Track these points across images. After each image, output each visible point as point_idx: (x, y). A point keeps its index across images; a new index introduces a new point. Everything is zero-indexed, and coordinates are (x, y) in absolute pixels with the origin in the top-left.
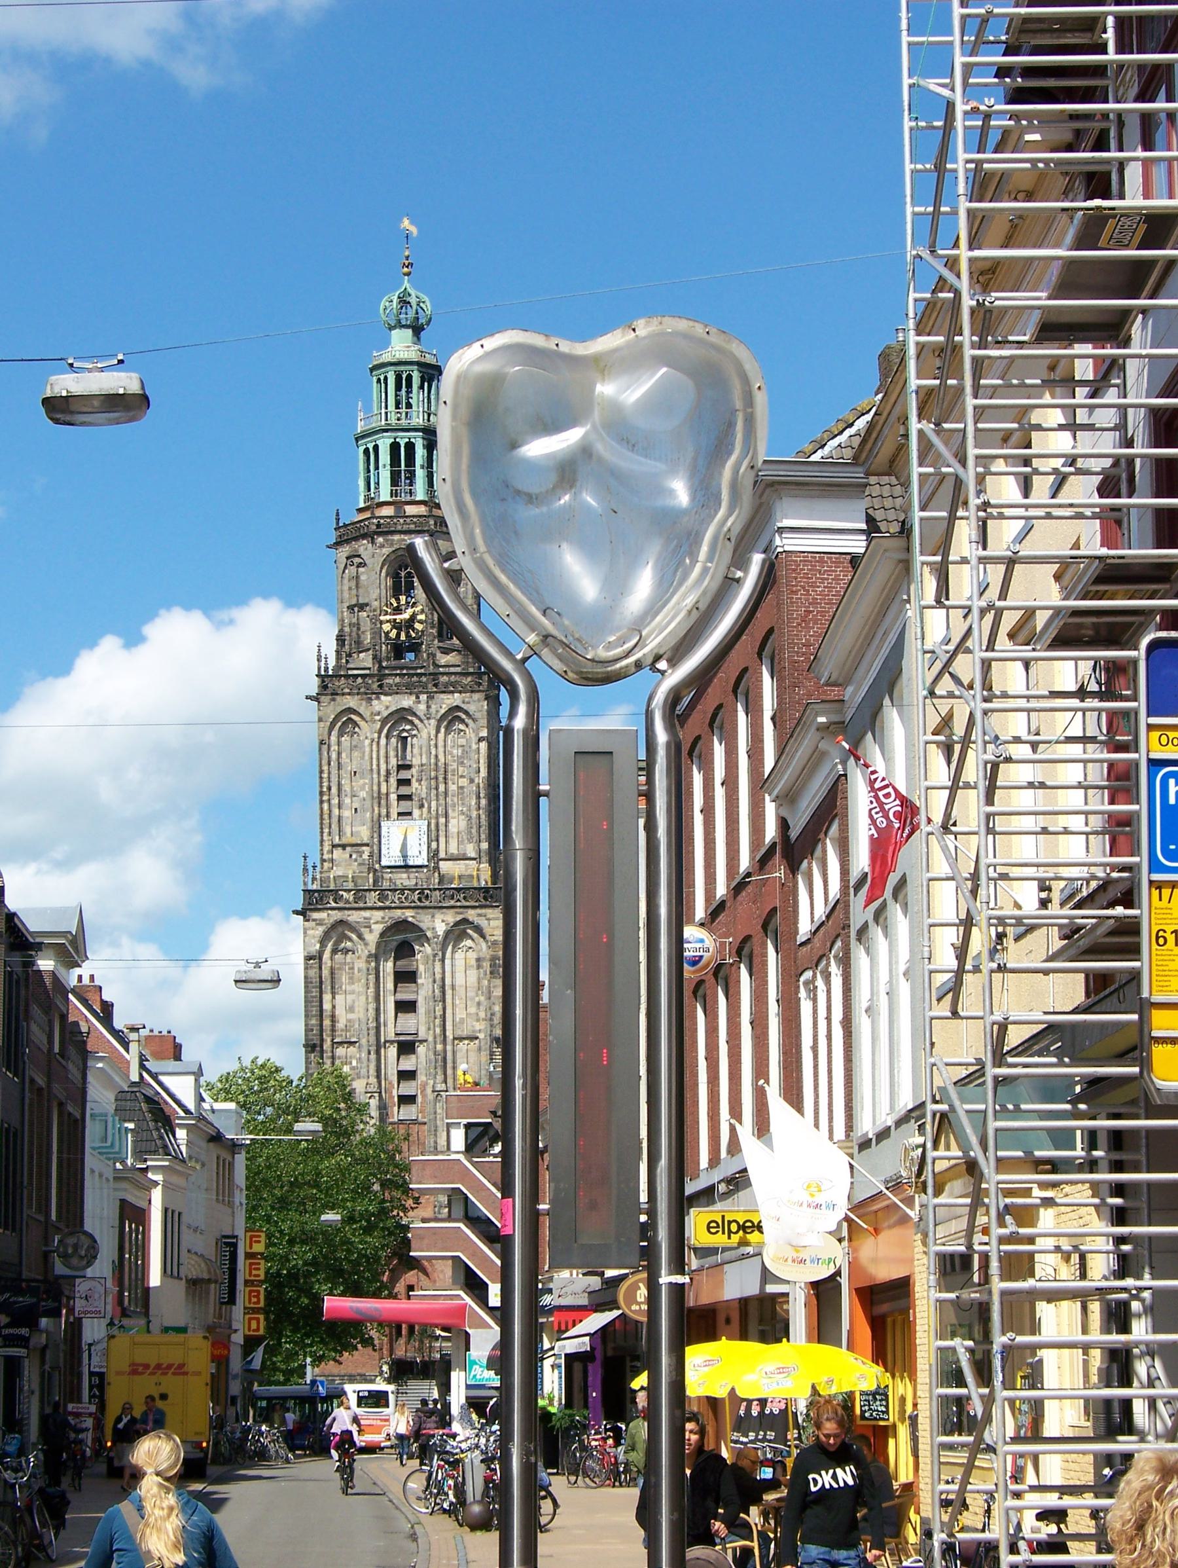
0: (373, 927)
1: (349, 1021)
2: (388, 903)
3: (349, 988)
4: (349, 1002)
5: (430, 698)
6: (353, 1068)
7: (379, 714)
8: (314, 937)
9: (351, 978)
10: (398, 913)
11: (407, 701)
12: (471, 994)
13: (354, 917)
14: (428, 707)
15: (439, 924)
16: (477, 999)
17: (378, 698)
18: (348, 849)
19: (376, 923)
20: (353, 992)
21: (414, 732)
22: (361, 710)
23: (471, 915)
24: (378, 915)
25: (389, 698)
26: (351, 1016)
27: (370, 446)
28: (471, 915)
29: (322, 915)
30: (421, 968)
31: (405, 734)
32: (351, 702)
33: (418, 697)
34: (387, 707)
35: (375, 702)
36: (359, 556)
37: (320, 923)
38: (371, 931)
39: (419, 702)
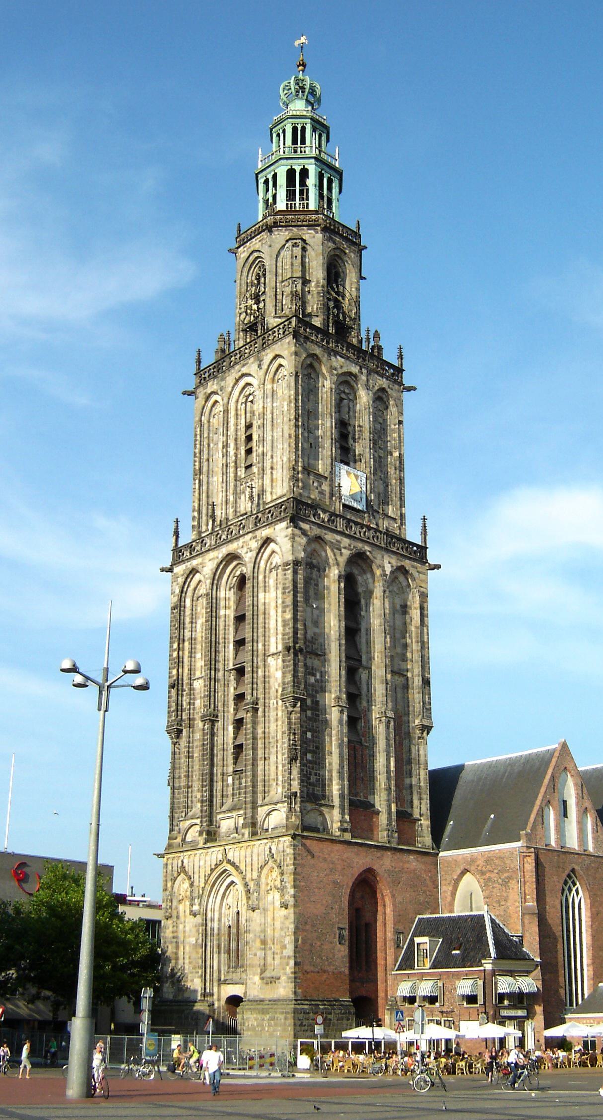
0: (343, 550)
2: (352, 533)
5: (368, 374)
6: (317, 680)
7: (336, 369)
8: (300, 544)
11: (355, 369)
13: (329, 537)
14: (367, 380)
15: (387, 564)
17: (335, 356)
19: (345, 548)
23: (407, 564)
24: (346, 541)
27: (298, 169)
28: (407, 564)
29: (306, 526)
31: (343, 396)
32: (318, 351)
34: (341, 367)
36: (304, 241)
37: (304, 533)
38: (341, 554)
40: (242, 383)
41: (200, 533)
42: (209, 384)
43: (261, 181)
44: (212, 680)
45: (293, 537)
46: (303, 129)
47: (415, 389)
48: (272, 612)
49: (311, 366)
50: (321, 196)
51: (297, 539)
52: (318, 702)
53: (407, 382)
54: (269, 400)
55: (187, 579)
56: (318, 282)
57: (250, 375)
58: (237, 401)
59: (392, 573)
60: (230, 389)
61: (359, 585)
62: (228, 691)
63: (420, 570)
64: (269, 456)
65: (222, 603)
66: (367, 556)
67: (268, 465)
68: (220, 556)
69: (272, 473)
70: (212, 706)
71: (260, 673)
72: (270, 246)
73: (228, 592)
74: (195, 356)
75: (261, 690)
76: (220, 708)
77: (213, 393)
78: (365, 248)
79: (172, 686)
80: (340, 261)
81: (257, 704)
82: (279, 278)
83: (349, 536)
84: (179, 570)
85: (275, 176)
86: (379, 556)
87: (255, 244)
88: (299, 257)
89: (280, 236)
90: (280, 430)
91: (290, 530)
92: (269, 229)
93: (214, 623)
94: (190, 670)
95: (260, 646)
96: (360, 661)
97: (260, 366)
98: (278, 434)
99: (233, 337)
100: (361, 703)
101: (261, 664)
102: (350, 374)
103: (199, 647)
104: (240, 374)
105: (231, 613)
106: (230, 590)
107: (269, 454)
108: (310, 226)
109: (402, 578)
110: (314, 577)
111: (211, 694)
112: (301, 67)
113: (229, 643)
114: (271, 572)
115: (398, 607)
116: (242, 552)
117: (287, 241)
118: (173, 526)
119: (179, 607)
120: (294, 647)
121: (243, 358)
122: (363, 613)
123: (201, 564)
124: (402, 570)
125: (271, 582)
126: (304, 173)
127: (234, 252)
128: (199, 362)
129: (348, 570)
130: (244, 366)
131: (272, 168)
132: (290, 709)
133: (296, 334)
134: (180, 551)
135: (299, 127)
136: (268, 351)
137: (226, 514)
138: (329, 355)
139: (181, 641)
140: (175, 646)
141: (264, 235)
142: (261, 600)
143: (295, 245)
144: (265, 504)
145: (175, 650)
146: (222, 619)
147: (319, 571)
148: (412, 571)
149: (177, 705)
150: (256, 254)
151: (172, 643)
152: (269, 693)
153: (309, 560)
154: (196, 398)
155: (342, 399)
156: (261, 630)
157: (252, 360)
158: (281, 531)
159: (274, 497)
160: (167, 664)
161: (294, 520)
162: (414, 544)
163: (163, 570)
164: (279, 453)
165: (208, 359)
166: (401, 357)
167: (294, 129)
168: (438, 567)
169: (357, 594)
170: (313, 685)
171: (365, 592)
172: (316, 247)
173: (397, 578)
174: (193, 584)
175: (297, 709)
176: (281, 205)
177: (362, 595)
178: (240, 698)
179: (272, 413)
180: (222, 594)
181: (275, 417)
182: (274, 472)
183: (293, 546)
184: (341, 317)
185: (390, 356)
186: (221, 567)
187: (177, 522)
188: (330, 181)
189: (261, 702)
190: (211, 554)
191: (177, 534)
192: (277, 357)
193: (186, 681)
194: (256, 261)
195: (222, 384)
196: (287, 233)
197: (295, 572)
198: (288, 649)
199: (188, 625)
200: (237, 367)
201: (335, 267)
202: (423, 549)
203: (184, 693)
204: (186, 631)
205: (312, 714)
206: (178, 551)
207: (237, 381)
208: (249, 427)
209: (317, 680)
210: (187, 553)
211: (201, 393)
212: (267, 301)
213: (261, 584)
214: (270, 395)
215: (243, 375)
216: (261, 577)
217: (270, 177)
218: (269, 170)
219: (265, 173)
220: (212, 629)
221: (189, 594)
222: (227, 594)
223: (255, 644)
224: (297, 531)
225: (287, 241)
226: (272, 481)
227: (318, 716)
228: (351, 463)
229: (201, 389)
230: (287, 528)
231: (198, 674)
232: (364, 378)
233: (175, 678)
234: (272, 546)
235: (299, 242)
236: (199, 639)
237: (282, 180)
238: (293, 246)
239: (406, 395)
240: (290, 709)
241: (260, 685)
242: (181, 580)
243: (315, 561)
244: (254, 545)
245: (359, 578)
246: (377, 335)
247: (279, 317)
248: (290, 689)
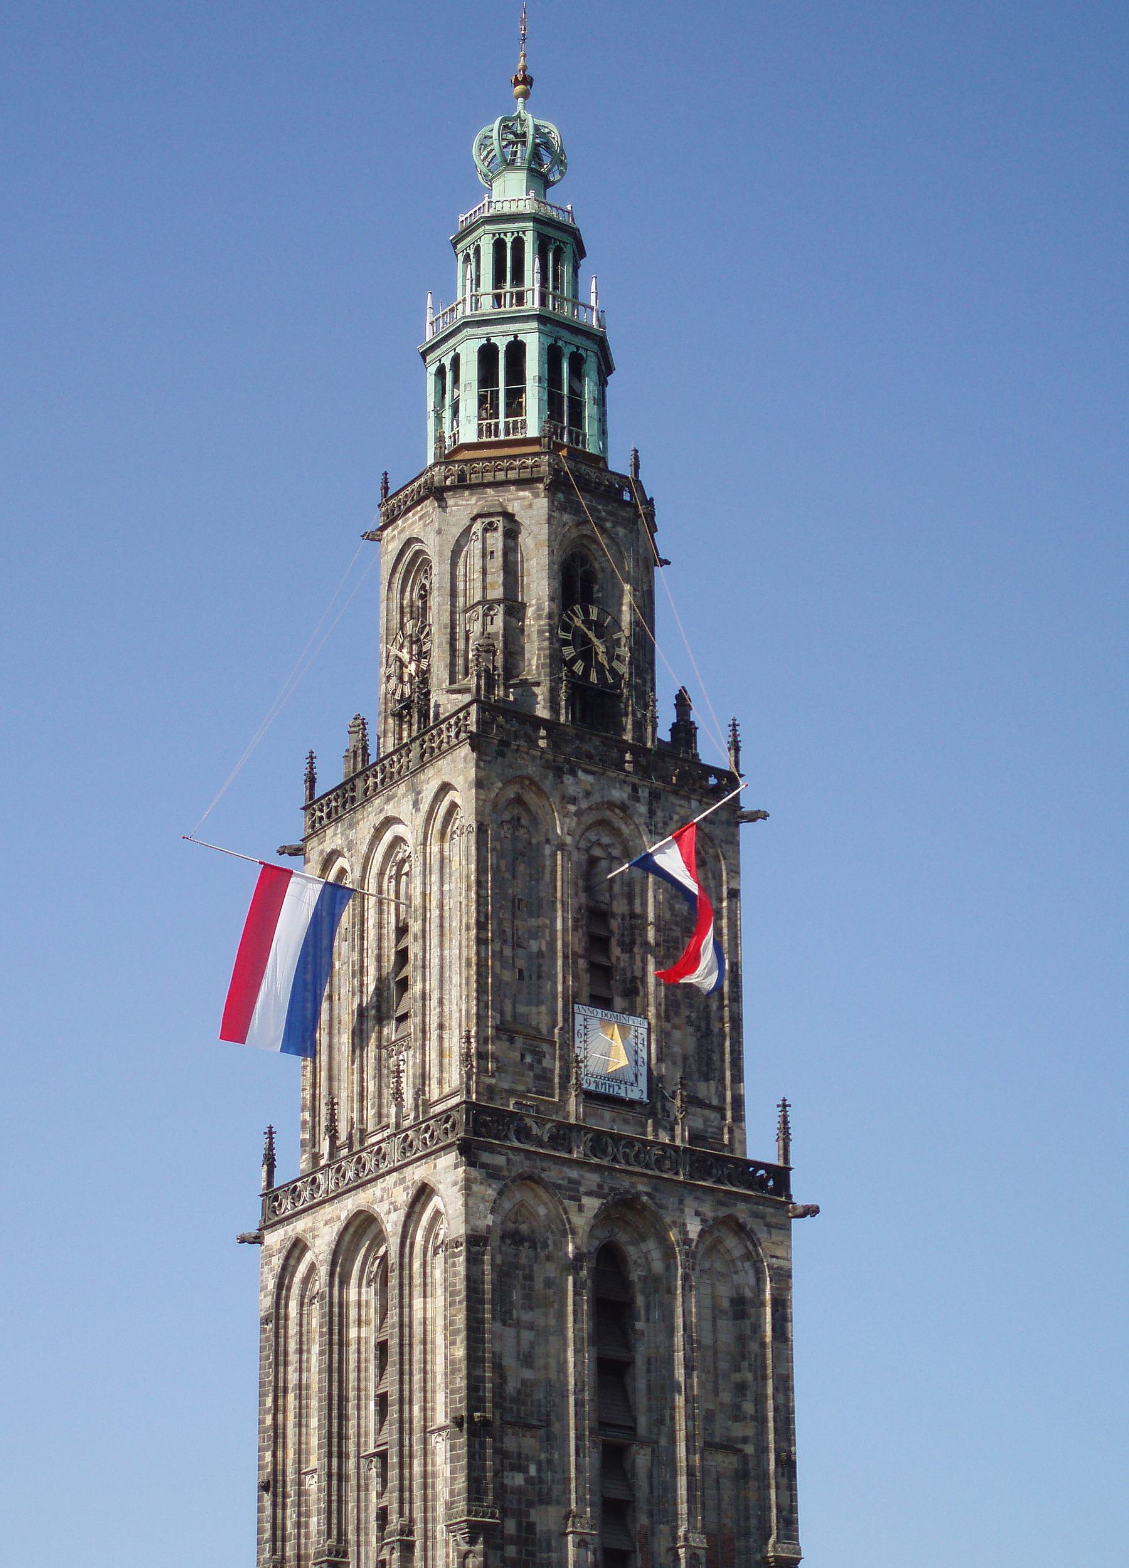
0: (585, 1200)
1: (524, 1383)
3: (526, 1317)
4: (525, 1344)
5: (655, 796)
6: (529, 1481)
7: (573, 800)
9: (527, 1297)
10: (625, 1183)
12: (723, 1366)
16: (736, 1377)
17: (573, 773)
18: (519, 1040)
19: (589, 1194)
20: (531, 1327)
21: (616, 852)
22: (547, 785)
23: (741, 1211)
24: (592, 1179)
25: (590, 778)
26: (527, 1374)
27: (502, 343)
29: (500, 1160)
30: (640, 1300)
31: (597, 852)
33: (635, 789)
34: (588, 794)
35: (568, 779)
36: (509, 517)
38: (581, 1208)
39: (638, 800)
40: (388, 837)
41: (316, 1157)
42: (329, 832)
43: (433, 369)
44: (336, 1478)
45: (468, 1186)
46: (518, 244)
47: (765, 816)
48: (440, 1340)
49: (519, 800)
50: (553, 402)
51: (475, 1188)
52: (531, 1527)
54: (435, 878)
55: (287, 1258)
56: (539, 608)
57: (398, 821)
58: (381, 874)
59: (701, 1234)
60: (364, 849)
61: (632, 1267)
62: (367, 1500)
63: (773, 1220)
64: (434, 1002)
65: (353, 1314)
66: (645, 1207)
67: (433, 1021)
68: (344, 1215)
69: (441, 1038)
70: (335, 1532)
71: (417, 1468)
72: (439, 532)
73: (364, 1290)
74: (304, 770)
75: (418, 1504)
76: (351, 1537)
77: (334, 855)
79: (264, 1487)
80: (593, 547)
81: (411, 1533)
82: (461, 601)
83: (597, 1168)
84: (275, 1239)
85: (456, 361)
86: (672, 1202)
87: (412, 524)
88: (499, 554)
89: (463, 507)
90: (455, 943)
91: (461, 1170)
92: (438, 493)
93: (336, 1356)
94: (299, 1452)
95: (416, 1409)
96: (633, 1429)
97: (416, 804)
98: (453, 951)
99: (372, 732)
100: (634, 1519)
101: (417, 1448)
102: (611, 805)
103: (314, 1403)
104: (382, 817)
105: (370, 1334)
106: (368, 1285)
107: (435, 996)
108: (521, 483)
109: (731, 1242)
110: (523, 1261)
111: (335, 1509)
112: (520, 88)
113: (367, 1398)
114: (435, 1253)
115: (725, 1304)
116: (381, 1209)
117: (474, 519)
118: (264, 1142)
119: (276, 1317)
120: (470, 1417)
121: (390, 780)
122: (640, 1325)
123: (312, 1230)
125: (438, 1274)
126: (517, 350)
127: (374, 537)
128: (311, 780)
129: (603, 1234)
130: (389, 799)
131: (451, 342)
132: (465, 1547)
133: (477, 742)
134: (276, 1199)
135: (509, 240)
136: (430, 772)
137: (361, 1121)
138: (559, 772)
139: (279, 1391)
140: (269, 1401)
141: (430, 505)
142: (418, 1315)
143: (489, 528)
144: (428, 1104)
145: (267, 1411)
146: (353, 1347)
147: (533, 1246)
148: (752, 1224)
149: (274, 1527)
150: (416, 547)
151: (262, 1395)
152: (434, 1509)
153: (510, 1225)
154: (306, 861)
155: (593, 861)
156: (417, 1377)
157: (402, 789)
158: (446, 1173)
159: (447, 1090)
160: (255, 1440)
161: (468, 1151)
162: (759, 1165)
164: (455, 993)
165: (330, 777)
166: (735, 746)
167: (499, 245)
168: (811, 1211)
169: (627, 1285)
170: (519, 1491)
171: (644, 1279)
172: (535, 529)
173: (719, 1241)
174: (302, 1269)
175: (479, 1547)
176: (469, 433)
177: (638, 1286)
178: (383, 1515)
179: (441, 906)
180: (352, 1294)
181: (446, 914)
182: (446, 1036)
183: (466, 1204)
184: (593, 678)
185: (712, 750)
186: (347, 1238)
187: (270, 1133)
188: (577, 363)
189: (418, 1527)
190: (328, 1210)
191: (270, 1160)
192: (445, 788)
193: (291, 1476)
194: (414, 563)
195: (352, 834)
196: (473, 500)
197: (473, 1261)
198: (458, 1422)
199: (293, 1357)
200: (377, 802)
201: (584, 560)
202: (781, 1175)
203: (289, 1501)
204: (290, 1369)
205: (519, 1552)
206: (271, 1196)
207: (379, 832)
208: (402, 931)
209: (529, 1481)
210: (287, 1203)
211: (316, 851)
213: (418, 1280)
214: (436, 866)
215: (389, 821)
216: (417, 1265)
217: (447, 361)
218: (444, 347)
219: (438, 352)
220: (335, 1371)
221: (295, 1290)
222: (360, 1294)
223: (406, 1407)
224: (474, 1173)
225: (474, 519)
226: (441, 1055)
227: (532, 1554)
228: (618, 1002)
229: (314, 842)
230: (456, 1166)
231: (314, 1463)
232: (643, 809)
233: (269, 1469)
234: (436, 1202)
235: (499, 522)
236: (315, 1387)
237: (470, 371)
238: (485, 530)
240: (465, 1547)
241: (418, 1493)
242: (277, 1262)
243: (524, 1228)
244: (403, 1197)
245: (632, 1252)
246: (682, 703)
247: (459, 692)
248: (462, 1505)
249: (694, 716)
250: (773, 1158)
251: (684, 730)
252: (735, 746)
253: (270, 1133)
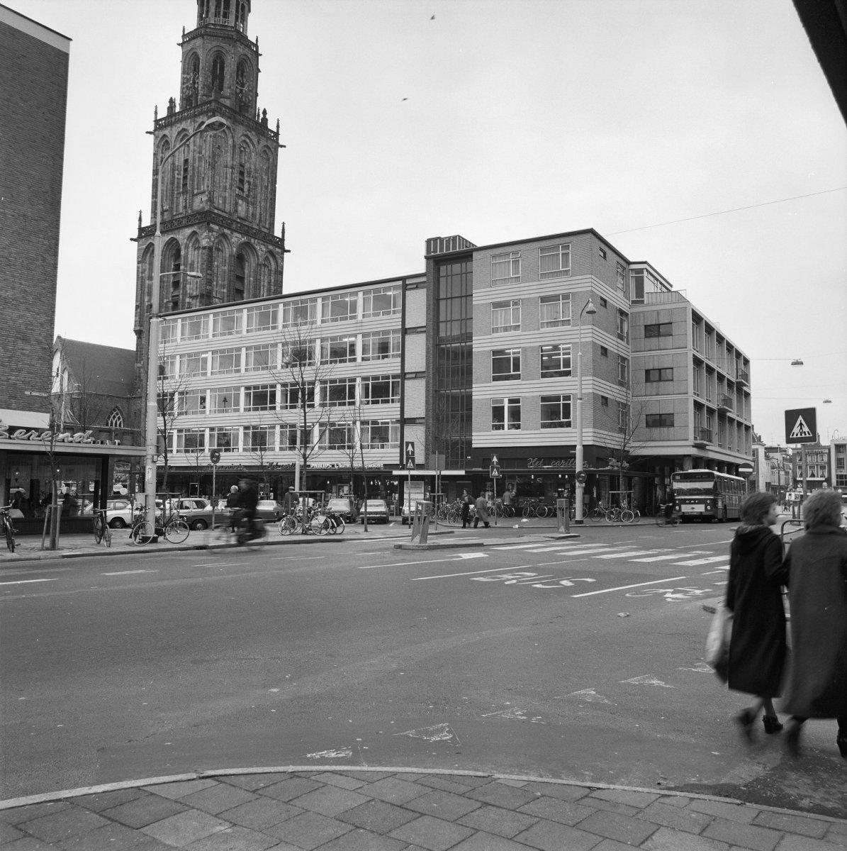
15: (261, 249)
31: (242, 149)
47: (285, 146)
53: (281, 142)
78: (261, 55)
124: (271, 252)
162: (278, 238)
163: (132, 239)
165: (163, 113)
166: (278, 127)
168: (289, 251)
185: (272, 126)
191: (140, 220)
206: (141, 230)
212: (200, 83)
239: (280, 149)
246: (265, 112)
249: (267, 117)
250: (280, 236)
251: (265, 120)
252: (278, 127)
253: (141, 212)
